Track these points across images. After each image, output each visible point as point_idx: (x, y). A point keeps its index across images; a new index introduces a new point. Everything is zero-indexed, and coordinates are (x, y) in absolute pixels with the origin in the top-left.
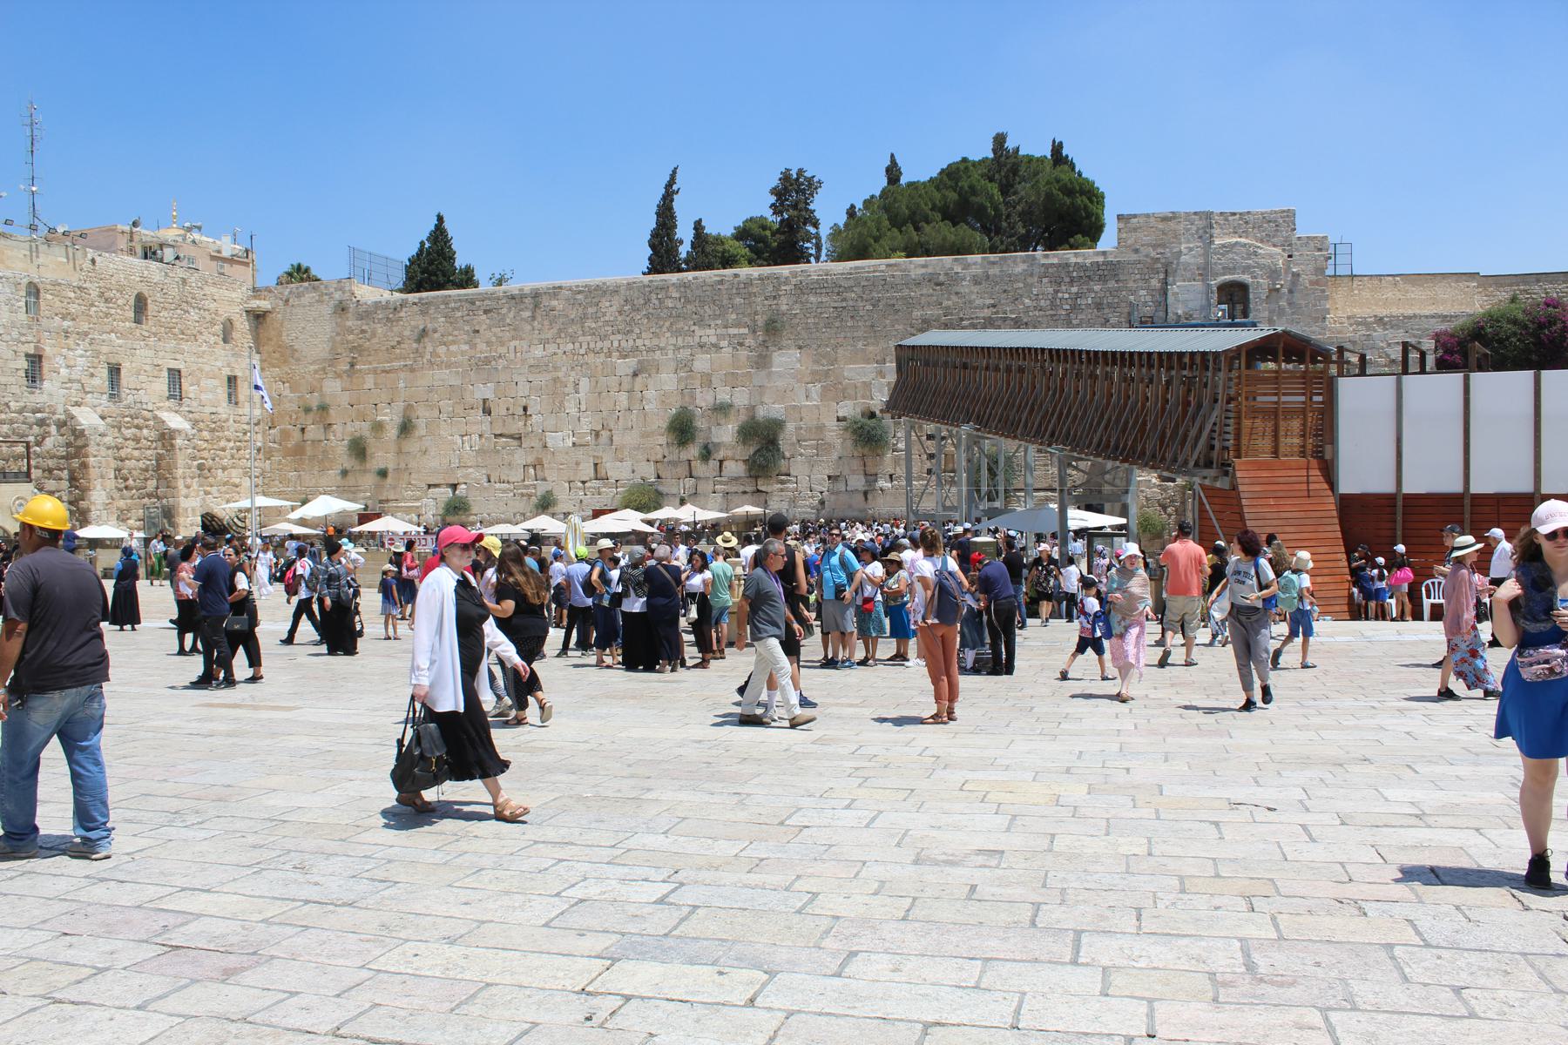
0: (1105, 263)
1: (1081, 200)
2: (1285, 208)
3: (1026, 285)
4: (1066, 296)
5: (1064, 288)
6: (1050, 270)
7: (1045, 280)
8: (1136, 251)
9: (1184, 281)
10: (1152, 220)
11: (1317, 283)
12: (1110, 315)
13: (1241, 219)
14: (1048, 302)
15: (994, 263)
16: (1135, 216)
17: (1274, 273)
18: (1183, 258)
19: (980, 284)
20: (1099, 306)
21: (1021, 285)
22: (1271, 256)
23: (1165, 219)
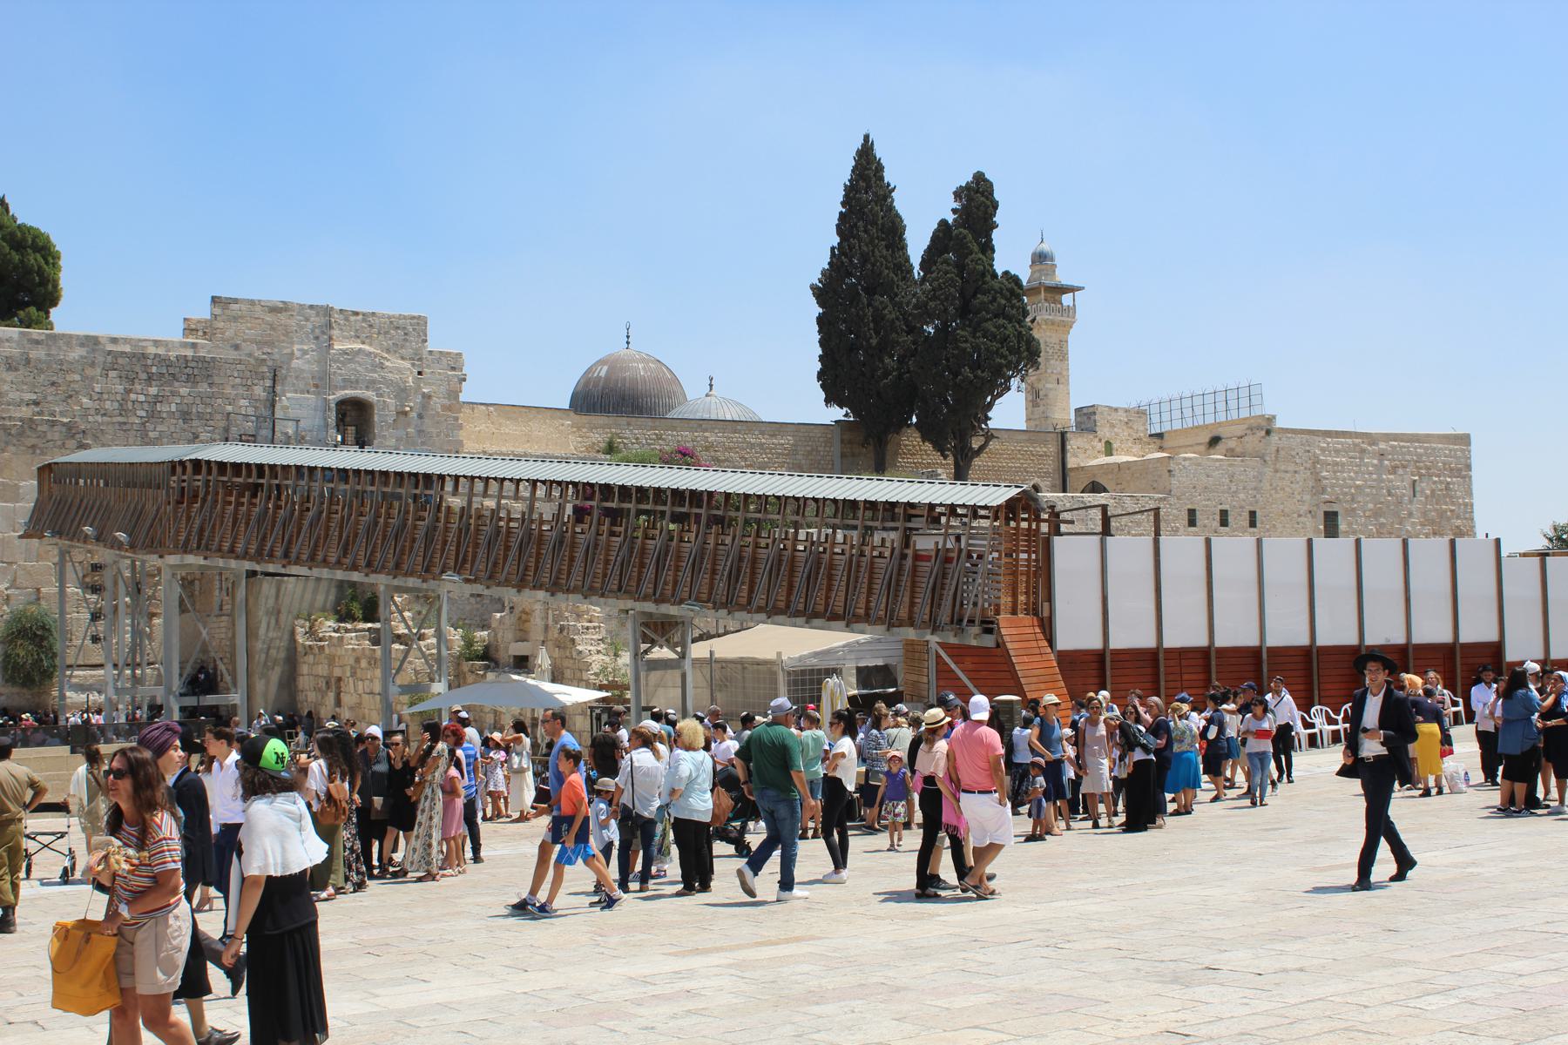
0: (196, 359)
1: (33, 259)
2: (416, 314)
3: (84, 378)
4: (142, 398)
5: (138, 387)
6: (120, 361)
7: (112, 374)
8: (237, 347)
9: (296, 392)
10: (258, 308)
11: (449, 408)
12: (200, 430)
13: (364, 320)
14: (116, 405)
15: (37, 342)
16: (236, 301)
17: (402, 392)
18: (295, 363)
19: (17, 370)
20: (185, 416)
21: (77, 377)
22: (400, 371)
23: (274, 310)
